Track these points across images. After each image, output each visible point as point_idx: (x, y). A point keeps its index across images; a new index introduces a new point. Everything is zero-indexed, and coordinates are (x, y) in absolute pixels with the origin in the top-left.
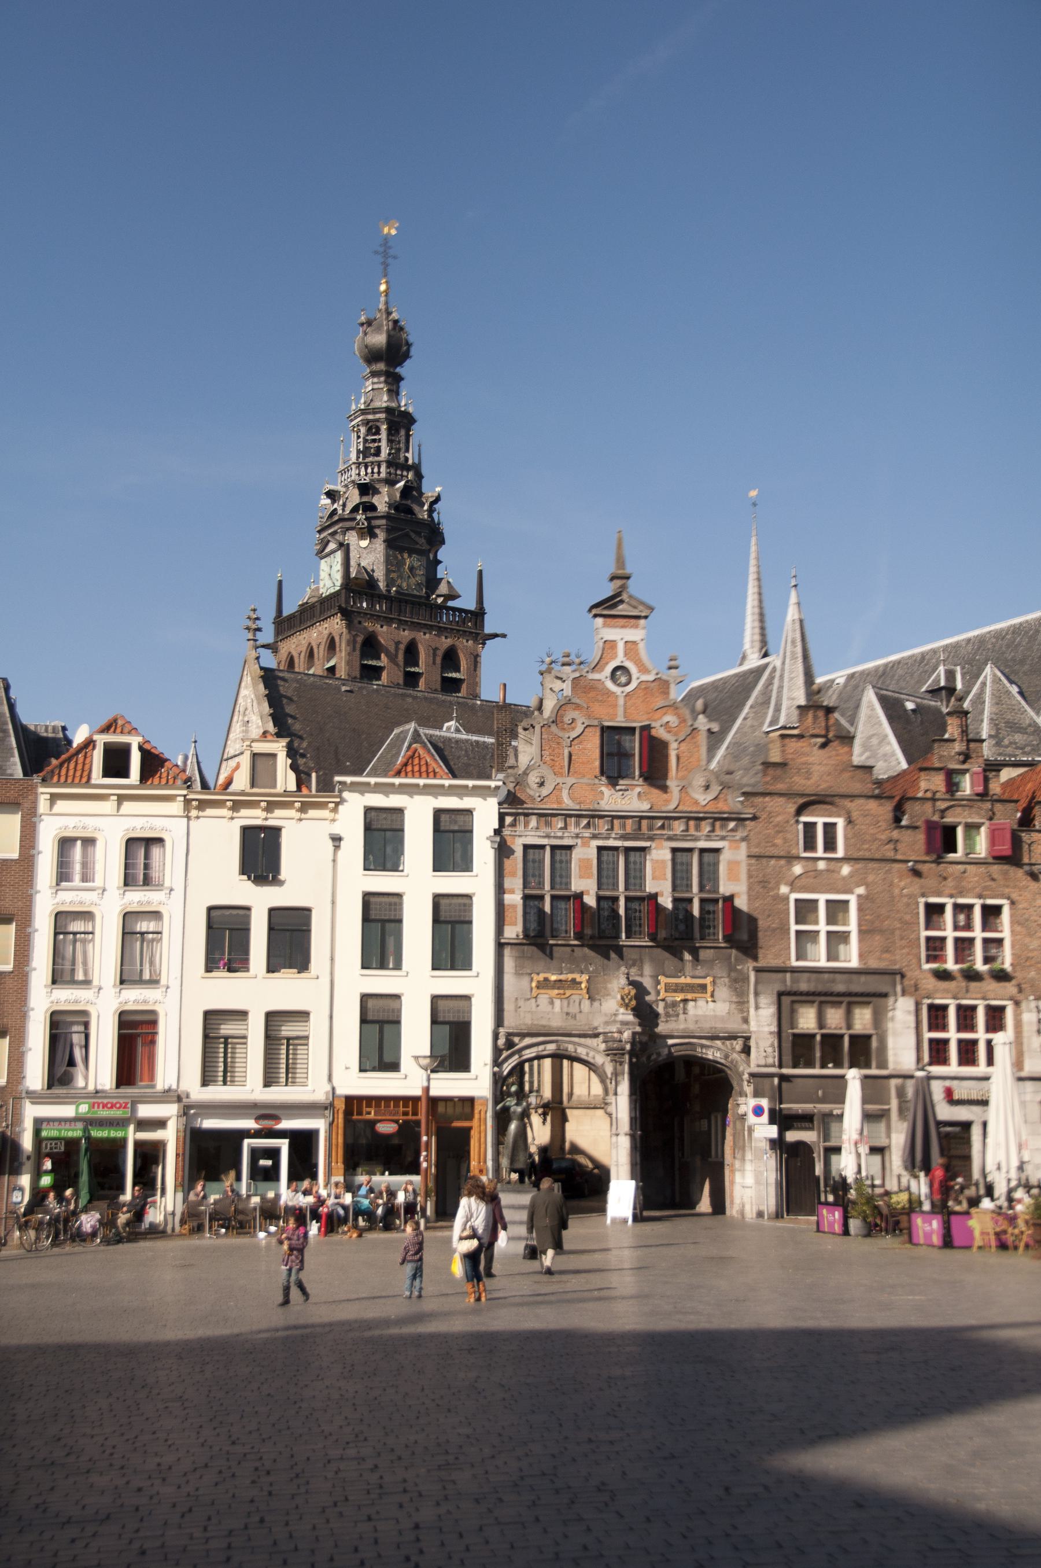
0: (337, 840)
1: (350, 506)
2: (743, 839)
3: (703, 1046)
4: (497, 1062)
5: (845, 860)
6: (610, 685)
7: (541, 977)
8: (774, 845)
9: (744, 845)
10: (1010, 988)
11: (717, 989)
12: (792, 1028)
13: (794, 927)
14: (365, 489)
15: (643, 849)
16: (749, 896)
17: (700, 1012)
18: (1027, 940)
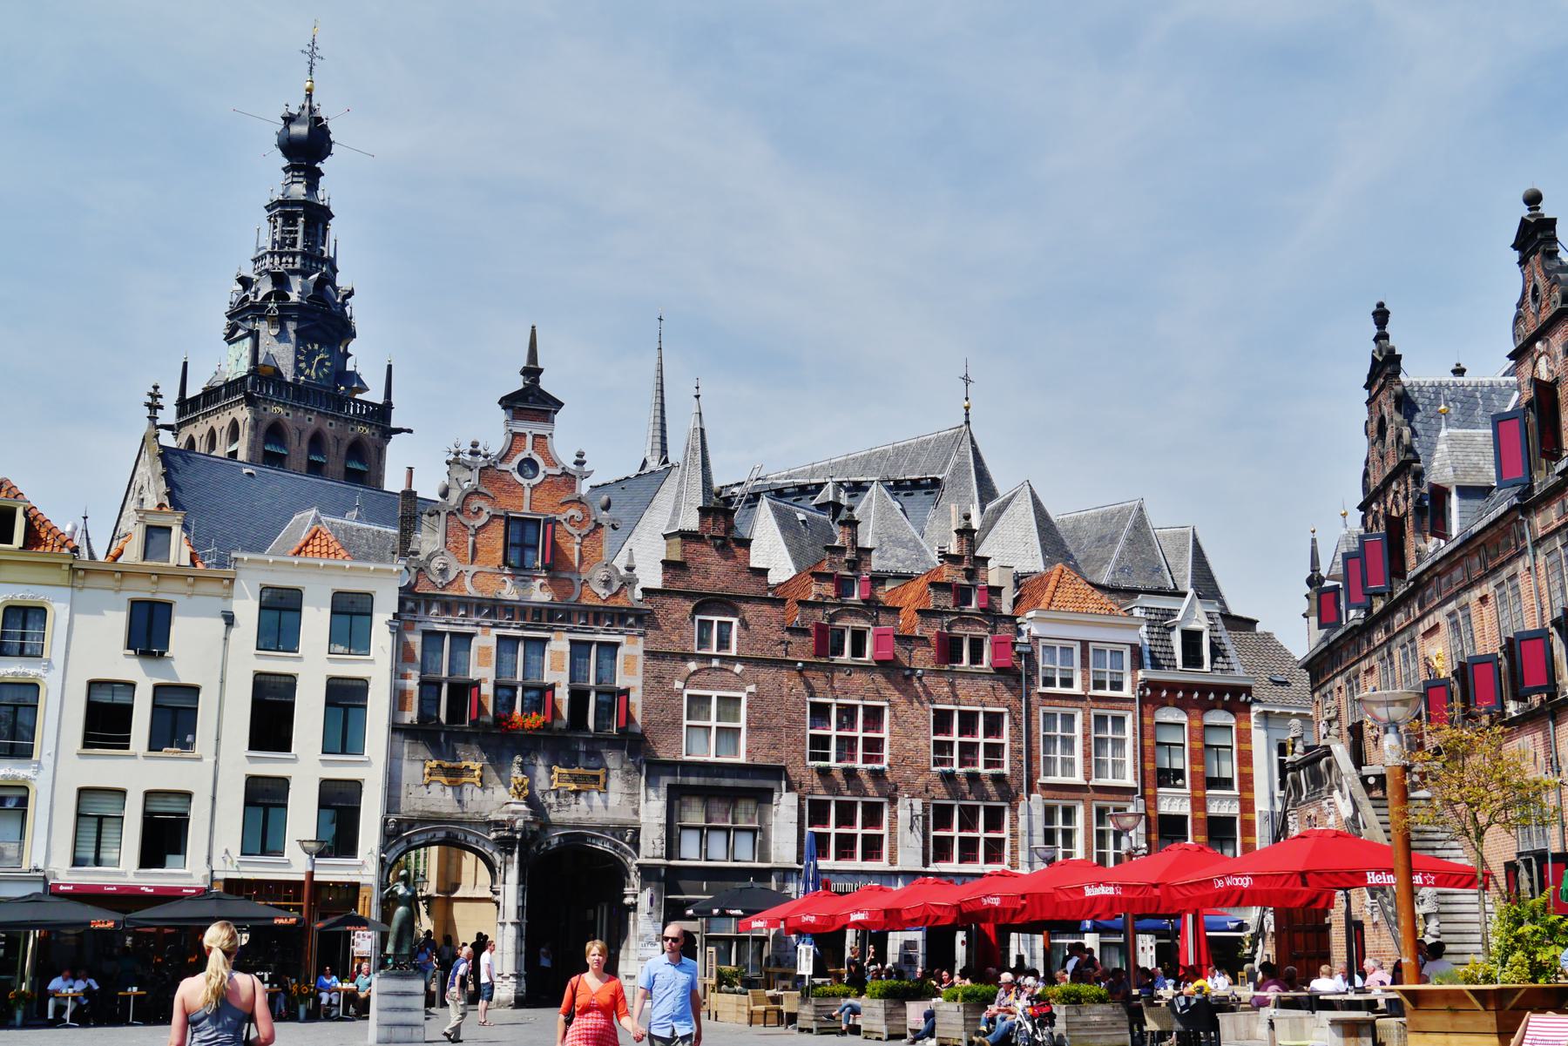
0: (229, 620)
1: (261, 295)
3: (593, 837)
4: (384, 848)
6: (517, 476)
13: (686, 722)
14: (280, 280)
15: (547, 640)
18: (904, 741)
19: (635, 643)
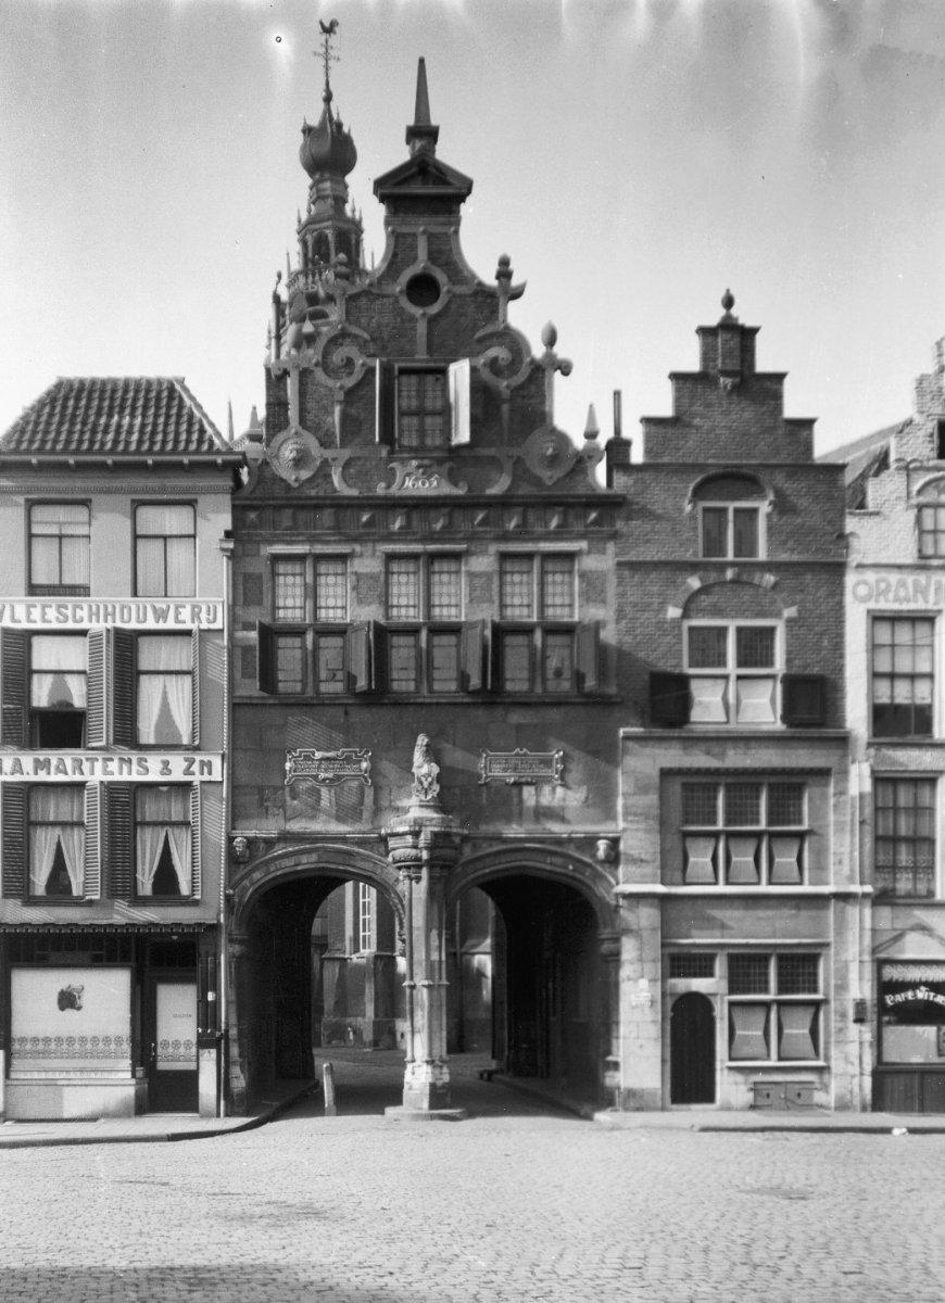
6: (405, 303)
19: (603, 552)
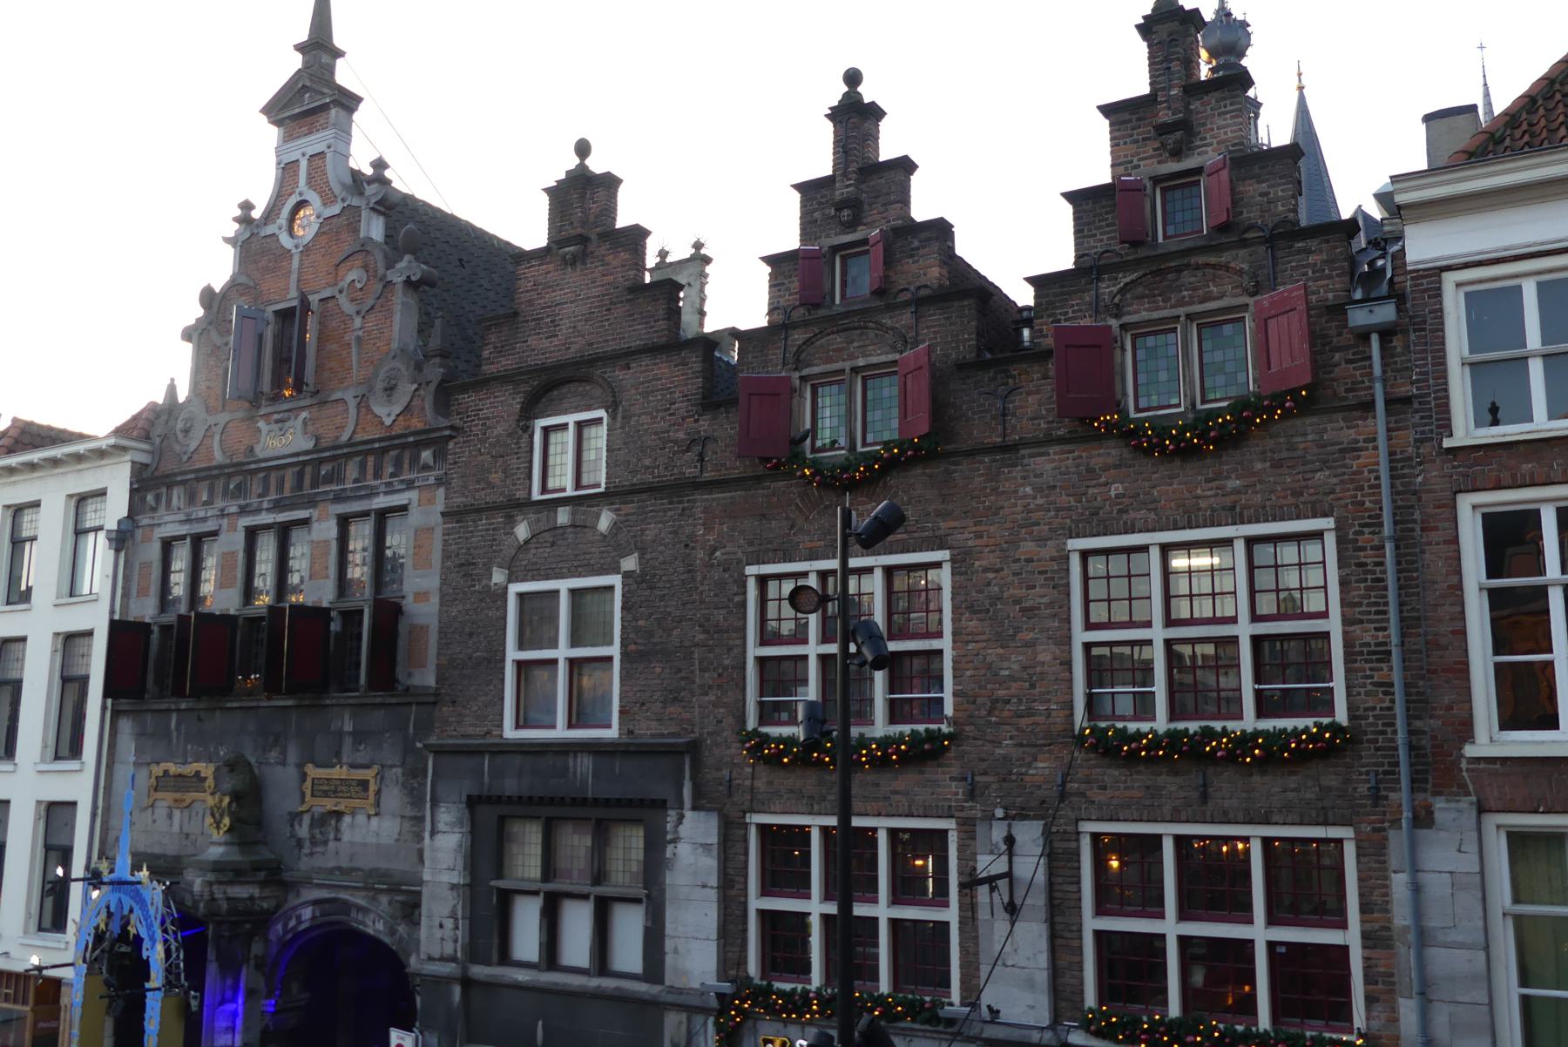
2: (440, 482)
5: (609, 497)
7: (158, 770)
8: (490, 485)
9: (441, 491)
10: (946, 781)
11: (385, 790)
12: (500, 876)
16: (442, 597)
17: (358, 838)
18: (993, 653)
